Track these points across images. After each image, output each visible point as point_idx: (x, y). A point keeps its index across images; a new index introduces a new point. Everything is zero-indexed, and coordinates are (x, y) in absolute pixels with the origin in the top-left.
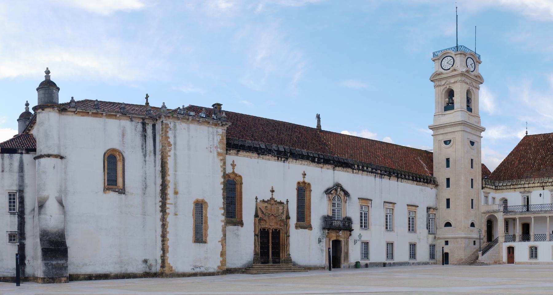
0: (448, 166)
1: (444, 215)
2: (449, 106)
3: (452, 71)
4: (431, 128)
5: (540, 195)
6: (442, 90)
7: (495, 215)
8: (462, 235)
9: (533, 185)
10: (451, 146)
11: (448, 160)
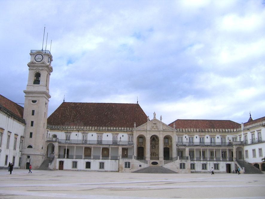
0: (33, 114)
1: (28, 141)
2: (37, 82)
3: (41, 63)
4: (25, 92)
5: (76, 135)
6: (34, 73)
7: (54, 143)
8: (38, 153)
9: (73, 129)
10: (36, 104)
11: (33, 111)
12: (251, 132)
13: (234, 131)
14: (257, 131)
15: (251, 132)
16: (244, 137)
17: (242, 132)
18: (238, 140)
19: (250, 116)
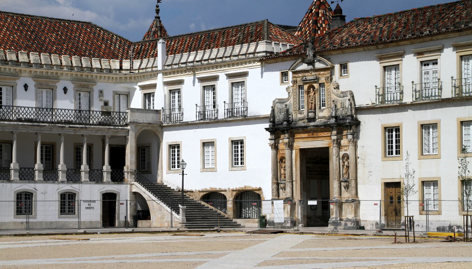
12: (202, 80)
13: (121, 68)
14: (230, 76)
15: (202, 80)
16: (167, 92)
17: (160, 75)
18: (137, 101)
19: (158, 11)
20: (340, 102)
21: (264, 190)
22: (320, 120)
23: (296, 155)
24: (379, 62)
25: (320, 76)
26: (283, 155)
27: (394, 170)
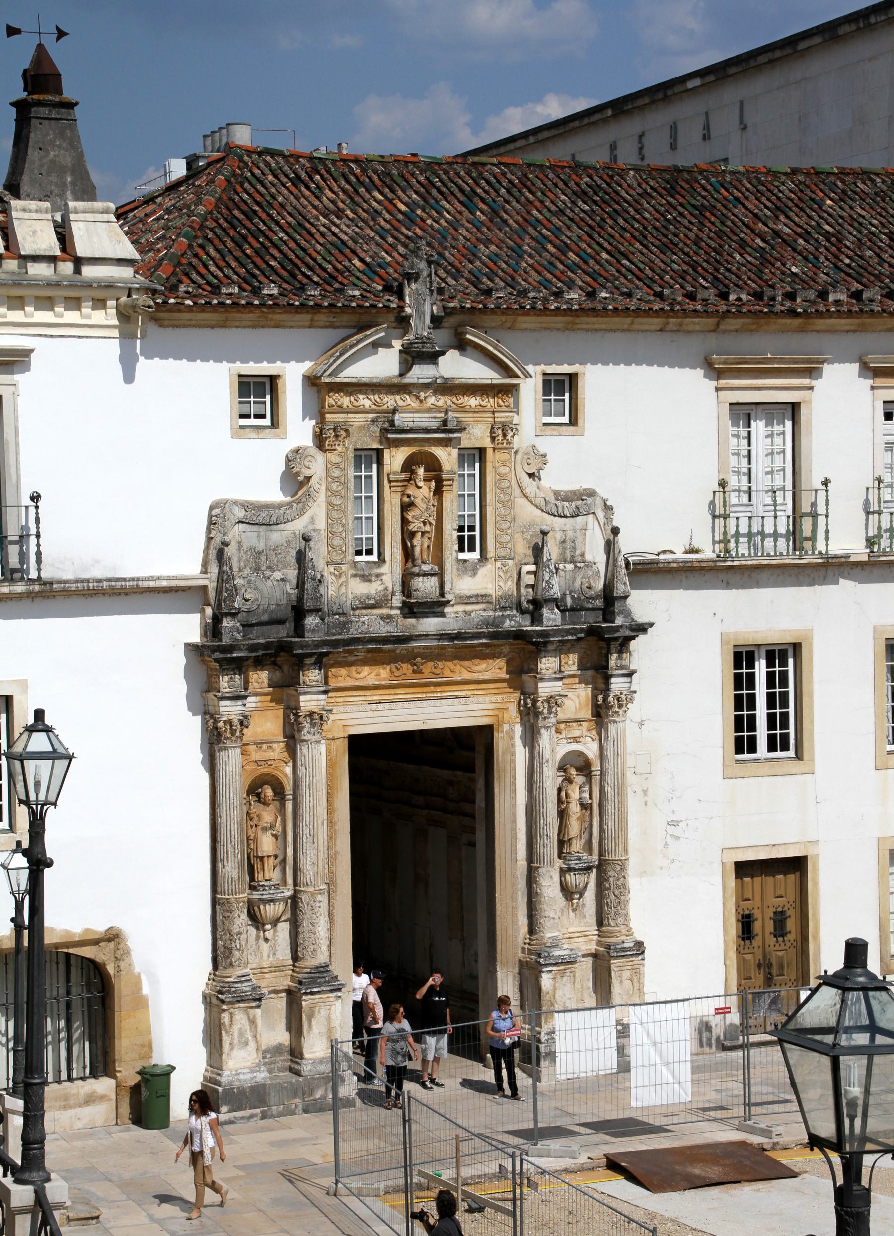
20: (559, 536)
21: (134, 942)
22: (460, 608)
23: (331, 765)
24: (714, 384)
25: (466, 417)
26: (265, 770)
27: (770, 811)
